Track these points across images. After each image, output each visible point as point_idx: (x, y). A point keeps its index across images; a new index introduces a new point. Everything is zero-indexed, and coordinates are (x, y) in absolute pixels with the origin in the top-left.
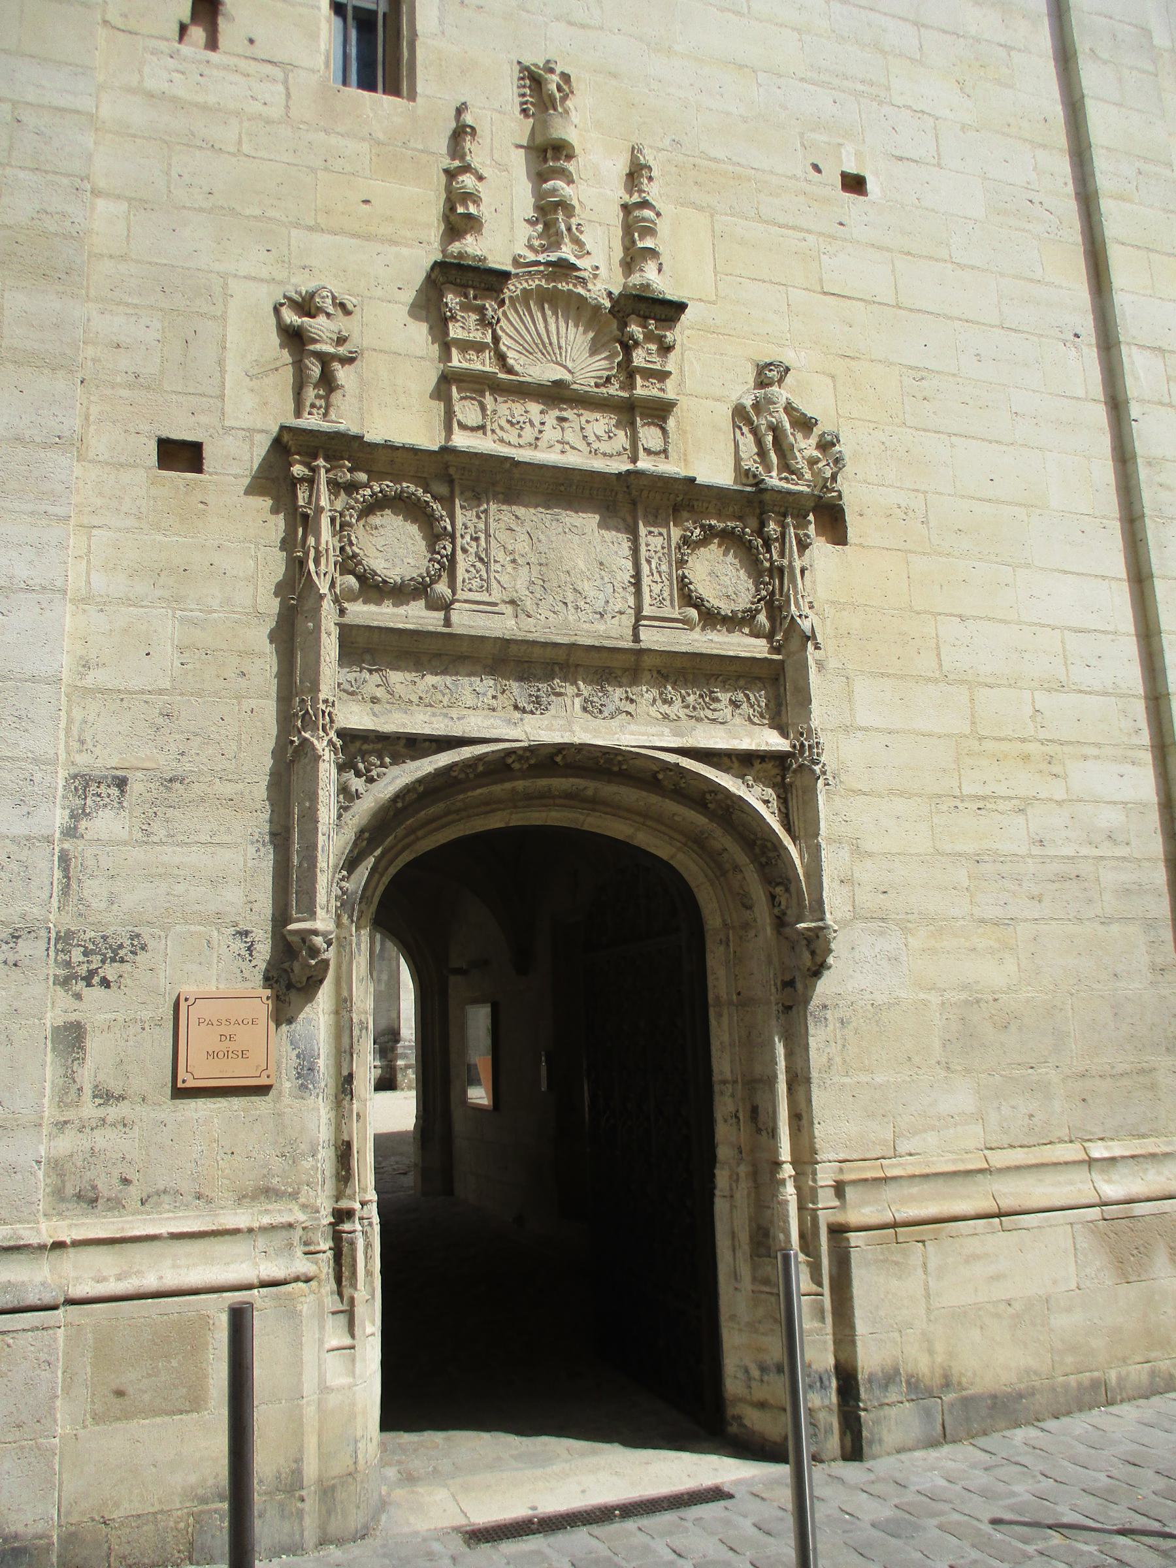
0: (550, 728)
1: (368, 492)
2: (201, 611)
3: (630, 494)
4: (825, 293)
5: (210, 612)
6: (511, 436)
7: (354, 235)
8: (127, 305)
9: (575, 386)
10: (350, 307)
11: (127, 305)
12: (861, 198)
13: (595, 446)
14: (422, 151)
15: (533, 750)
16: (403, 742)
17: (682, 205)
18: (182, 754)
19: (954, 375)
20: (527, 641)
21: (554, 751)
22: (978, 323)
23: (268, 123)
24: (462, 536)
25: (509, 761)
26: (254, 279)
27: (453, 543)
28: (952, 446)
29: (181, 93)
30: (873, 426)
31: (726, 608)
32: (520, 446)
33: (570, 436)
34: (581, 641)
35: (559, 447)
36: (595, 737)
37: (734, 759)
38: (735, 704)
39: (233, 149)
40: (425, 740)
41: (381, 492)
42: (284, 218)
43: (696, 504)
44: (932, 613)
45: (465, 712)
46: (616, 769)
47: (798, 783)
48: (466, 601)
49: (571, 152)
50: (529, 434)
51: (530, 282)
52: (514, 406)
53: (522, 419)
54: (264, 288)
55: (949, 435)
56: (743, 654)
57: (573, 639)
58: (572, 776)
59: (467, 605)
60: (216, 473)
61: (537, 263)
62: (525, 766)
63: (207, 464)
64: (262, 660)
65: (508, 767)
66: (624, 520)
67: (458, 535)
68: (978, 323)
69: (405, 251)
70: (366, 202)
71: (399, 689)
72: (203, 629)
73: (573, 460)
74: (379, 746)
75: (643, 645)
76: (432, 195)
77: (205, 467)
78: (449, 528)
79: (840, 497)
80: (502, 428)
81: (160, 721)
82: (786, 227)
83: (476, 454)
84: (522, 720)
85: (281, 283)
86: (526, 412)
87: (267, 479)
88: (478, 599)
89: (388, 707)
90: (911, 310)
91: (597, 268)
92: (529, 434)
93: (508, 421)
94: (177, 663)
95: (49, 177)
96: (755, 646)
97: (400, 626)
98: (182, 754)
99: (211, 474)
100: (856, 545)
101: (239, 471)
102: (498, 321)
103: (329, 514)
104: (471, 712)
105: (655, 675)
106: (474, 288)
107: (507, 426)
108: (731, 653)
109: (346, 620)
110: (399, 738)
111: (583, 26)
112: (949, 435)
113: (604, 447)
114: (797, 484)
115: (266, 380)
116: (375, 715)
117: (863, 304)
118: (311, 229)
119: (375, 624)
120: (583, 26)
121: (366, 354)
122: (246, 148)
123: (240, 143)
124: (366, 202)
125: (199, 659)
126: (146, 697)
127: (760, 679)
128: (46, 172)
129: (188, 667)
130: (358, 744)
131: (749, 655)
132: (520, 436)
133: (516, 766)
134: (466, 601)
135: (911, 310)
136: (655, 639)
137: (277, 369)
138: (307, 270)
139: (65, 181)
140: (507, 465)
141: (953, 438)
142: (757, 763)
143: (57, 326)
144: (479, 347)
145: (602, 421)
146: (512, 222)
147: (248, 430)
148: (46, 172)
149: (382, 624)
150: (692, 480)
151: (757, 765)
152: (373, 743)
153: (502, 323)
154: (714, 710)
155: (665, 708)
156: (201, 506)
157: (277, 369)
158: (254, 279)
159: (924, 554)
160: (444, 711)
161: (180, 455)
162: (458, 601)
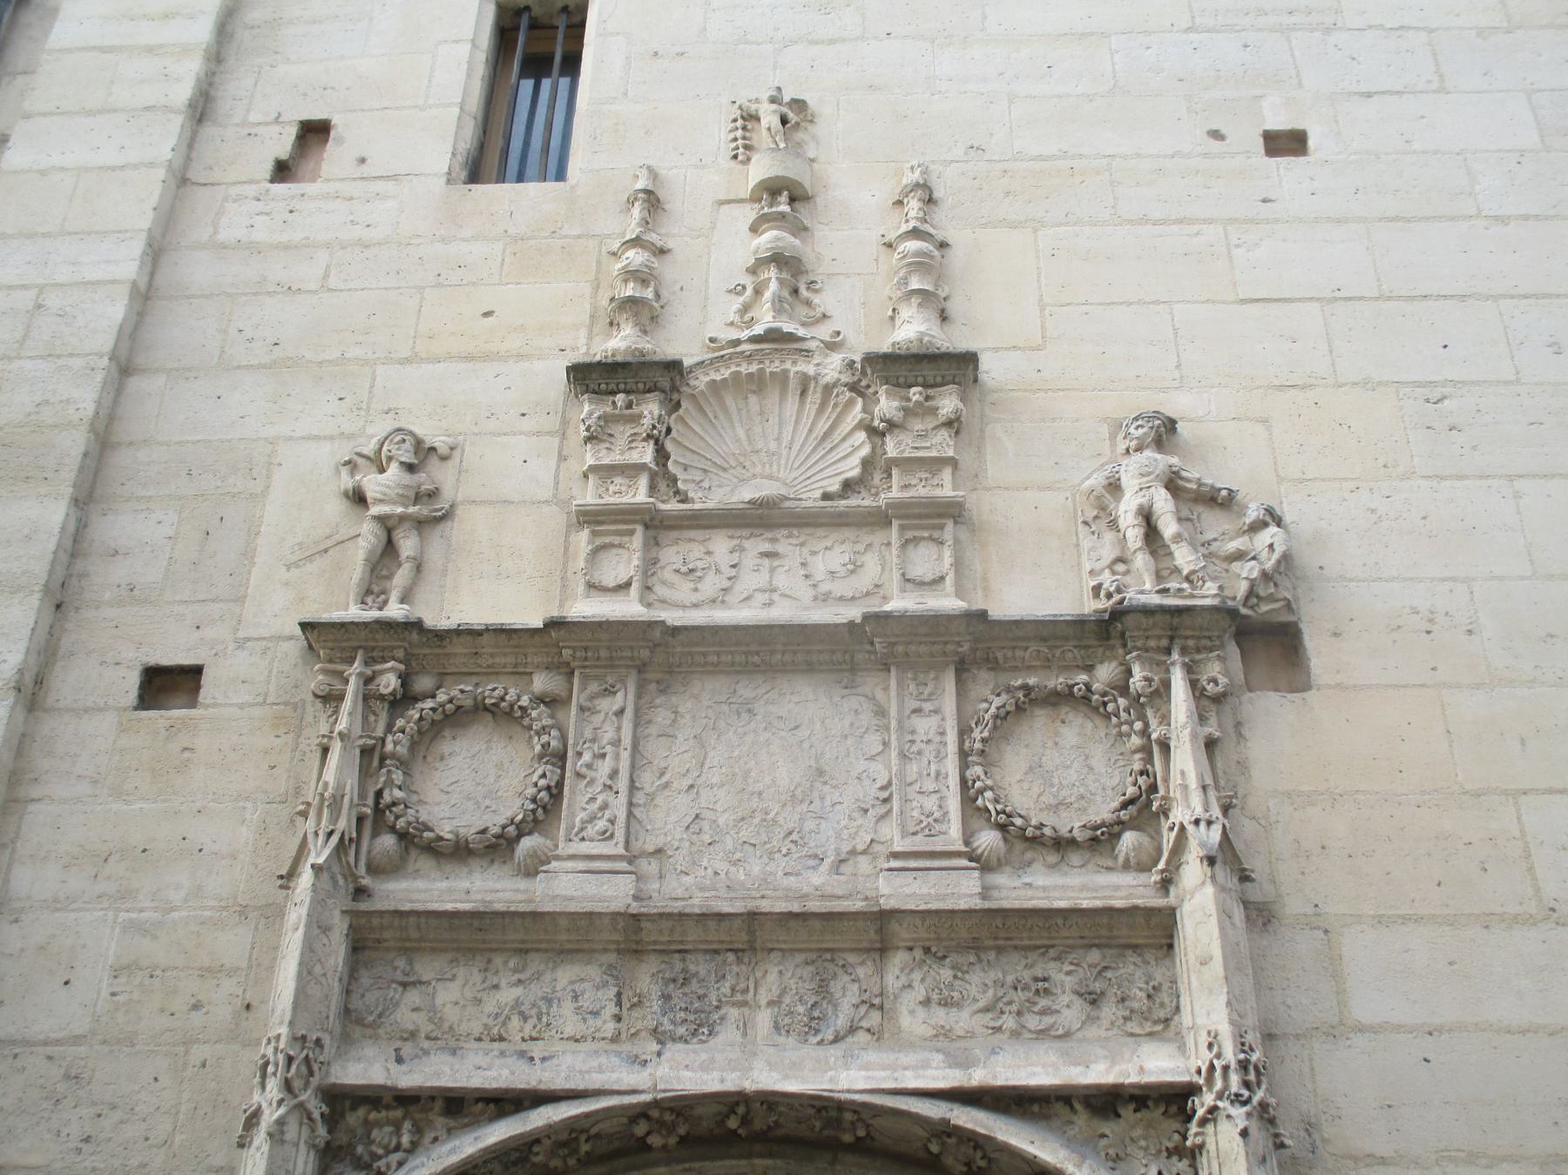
0: (705, 1068)
1: (429, 704)
2: (155, 909)
3: (875, 652)
4: (1244, 301)
5: (172, 909)
6: (683, 591)
7: (470, 358)
8: (138, 499)
9: (787, 504)
10: (443, 450)
11: (138, 499)
12: (1301, 159)
13: (824, 588)
14: (579, 237)
15: (679, 1108)
16: (439, 1104)
17: (984, 226)
18: (87, 1140)
19: (1506, 383)
20: (670, 915)
21: (724, 1109)
22: (1550, 296)
23: (367, 247)
24: (580, 754)
25: (640, 1129)
26: (316, 438)
27: (563, 768)
28: (1517, 496)
29: (259, 235)
30: (1352, 485)
31: (1071, 823)
32: (695, 606)
33: (781, 581)
34: (765, 906)
35: (761, 598)
36: (786, 1077)
37: (1078, 1106)
38: (1094, 1000)
39: (313, 286)
40: (478, 1100)
41: (451, 701)
42: (370, 355)
43: (999, 655)
44: (1506, 793)
45: (559, 1047)
46: (847, 1138)
47: (1211, 1146)
48: (573, 857)
49: (798, 193)
50: (711, 585)
51: (723, 370)
52: (684, 547)
53: (700, 564)
54: (325, 448)
55: (1510, 478)
56: (1085, 904)
57: (751, 905)
58: (762, 1156)
59: (570, 865)
60: (214, 705)
61: (737, 342)
62: (673, 1140)
63: (205, 694)
64: (235, 980)
65: (643, 1146)
66: (872, 698)
67: (570, 754)
68: (1550, 296)
69: (538, 365)
70: (488, 314)
71: (451, 1014)
72: (154, 937)
73: (781, 613)
74: (399, 1113)
75: (887, 904)
76: (587, 289)
77: (200, 699)
78: (554, 743)
79: (1288, 606)
80: (664, 583)
81: (61, 1088)
82: (1163, 222)
83: (600, 624)
84: (659, 1054)
85: (351, 437)
86: (709, 553)
87: (286, 704)
88: (594, 852)
89: (426, 1044)
90: (1411, 298)
91: (838, 333)
92: (711, 585)
93: (678, 571)
94: (105, 993)
95: (60, 362)
96: (1117, 888)
97: (449, 907)
98: (87, 1140)
99: (207, 707)
100: (1329, 687)
101: (248, 698)
102: (669, 431)
103: (361, 742)
104: (572, 1046)
105: (918, 953)
106: (627, 392)
107: (676, 579)
108: (1063, 904)
109: (363, 906)
110: (433, 1098)
111: (832, 42)
112: (1510, 478)
113: (841, 588)
114: (1192, 596)
115: (310, 567)
116: (399, 1060)
117: (1317, 305)
118: (406, 361)
119: (407, 907)
120: (832, 42)
121: (459, 511)
122: (333, 282)
123: (326, 276)
124: (488, 314)
125: (141, 984)
126: (49, 1050)
127: (1135, 947)
128: (59, 357)
129: (120, 998)
130: (361, 1112)
131: (1098, 903)
132: (696, 590)
133: (655, 1140)
134: (573, 857)
135: (1411, 298)
136: (907, 890)
137: (326, 551)
138: (392, 414)
139: (77, 363)
140: (657, 633)
141: (1520, 485)
142: (1127, 1112)
143: (28, 537)
144: (630, 471)
145: (838, 549)
146: (706, 299)
147: (271, 638)
148: (59, 357)
149: (419, 907)
150: (982, 615)
151: (1127, 1112)
152: (388, 1107)
153: (674, 434)
154: (1044, 1012)
155: (940, 1016)
156: (187, 754)
157: (326, 551)
158: (316, 438)
159: (1478, 686)
160: (524, 1046)
161: (168, 684)
162: (558, 858)
